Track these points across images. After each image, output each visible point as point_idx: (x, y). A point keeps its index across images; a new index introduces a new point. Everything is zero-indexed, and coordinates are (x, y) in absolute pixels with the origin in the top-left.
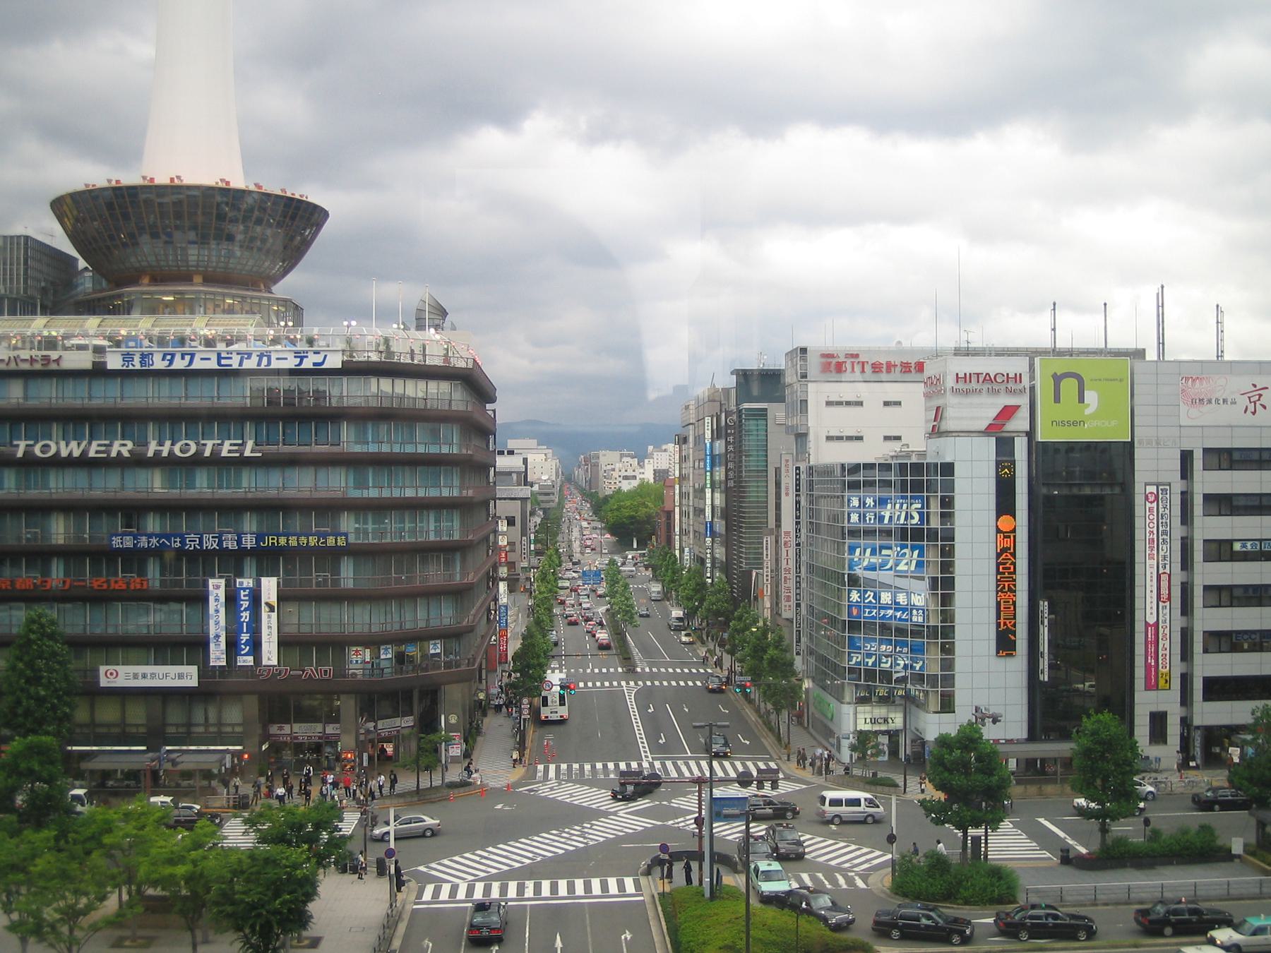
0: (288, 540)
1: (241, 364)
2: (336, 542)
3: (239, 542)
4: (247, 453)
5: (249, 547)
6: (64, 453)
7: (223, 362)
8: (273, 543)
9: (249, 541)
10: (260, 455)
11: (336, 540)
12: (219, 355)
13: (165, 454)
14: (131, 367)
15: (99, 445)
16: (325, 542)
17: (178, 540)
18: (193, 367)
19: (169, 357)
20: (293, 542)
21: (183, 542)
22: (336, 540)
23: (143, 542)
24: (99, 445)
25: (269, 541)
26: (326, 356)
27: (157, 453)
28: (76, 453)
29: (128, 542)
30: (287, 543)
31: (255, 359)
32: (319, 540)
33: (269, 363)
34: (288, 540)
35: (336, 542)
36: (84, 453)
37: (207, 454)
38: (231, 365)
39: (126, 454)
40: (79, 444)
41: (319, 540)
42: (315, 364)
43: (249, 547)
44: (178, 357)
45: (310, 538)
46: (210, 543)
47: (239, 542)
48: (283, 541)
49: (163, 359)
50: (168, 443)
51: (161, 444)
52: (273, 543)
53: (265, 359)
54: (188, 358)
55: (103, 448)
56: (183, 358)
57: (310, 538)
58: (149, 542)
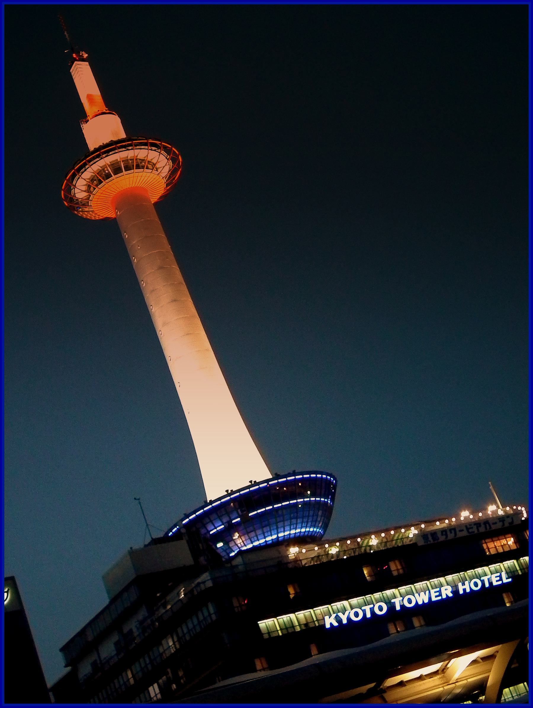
1: (478, 530)
4: (505, 581)
6: (420, 603)
7: (470, 530)
10: (510, 580)
12: (466, 526)
13: (468, 590)
14: (429, 543)
15: (435, 592)
18: (457, 536)
19: (444, 533)
24: (435, 592)
26: (512, 518)
27: (464, 590)
28: (426, 601)
31: (483, 526)
33: (490, 528)
36: (430, 598)
38: (474, 532)
39: (451, 595)
42: (510, 523)
44: (448, 533)
49: (442, 535)
50: (467, 583)
51: (463, 584)
53: (488, 527)
54: (453, 531)
55: (438, 594)
56: (451, 533)
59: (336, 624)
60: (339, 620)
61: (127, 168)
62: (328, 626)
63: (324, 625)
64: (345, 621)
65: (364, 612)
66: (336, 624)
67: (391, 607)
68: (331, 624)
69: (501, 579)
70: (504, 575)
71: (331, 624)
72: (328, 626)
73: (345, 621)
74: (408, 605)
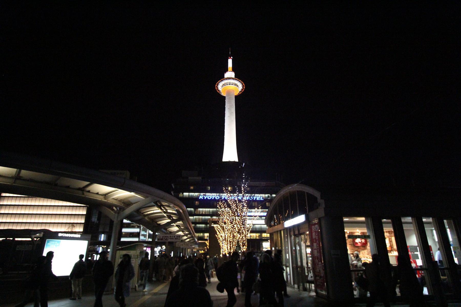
10: (263, 200)
37: (254, 199)
40: (233, 197)
59: (202, 198)
60: (204, 198)
61: (232, 84)
62: (200, 198)
63: (199, 198)
64: (205, 198)
65: (212, 197)
66: (202, 198)
67: (221, 198)
68: (201, 198)
69: (260, 199)
70: (261, 198)
71: (201, 198)
72: (200, 198)
73: (205, 198)
74: (216, 198)
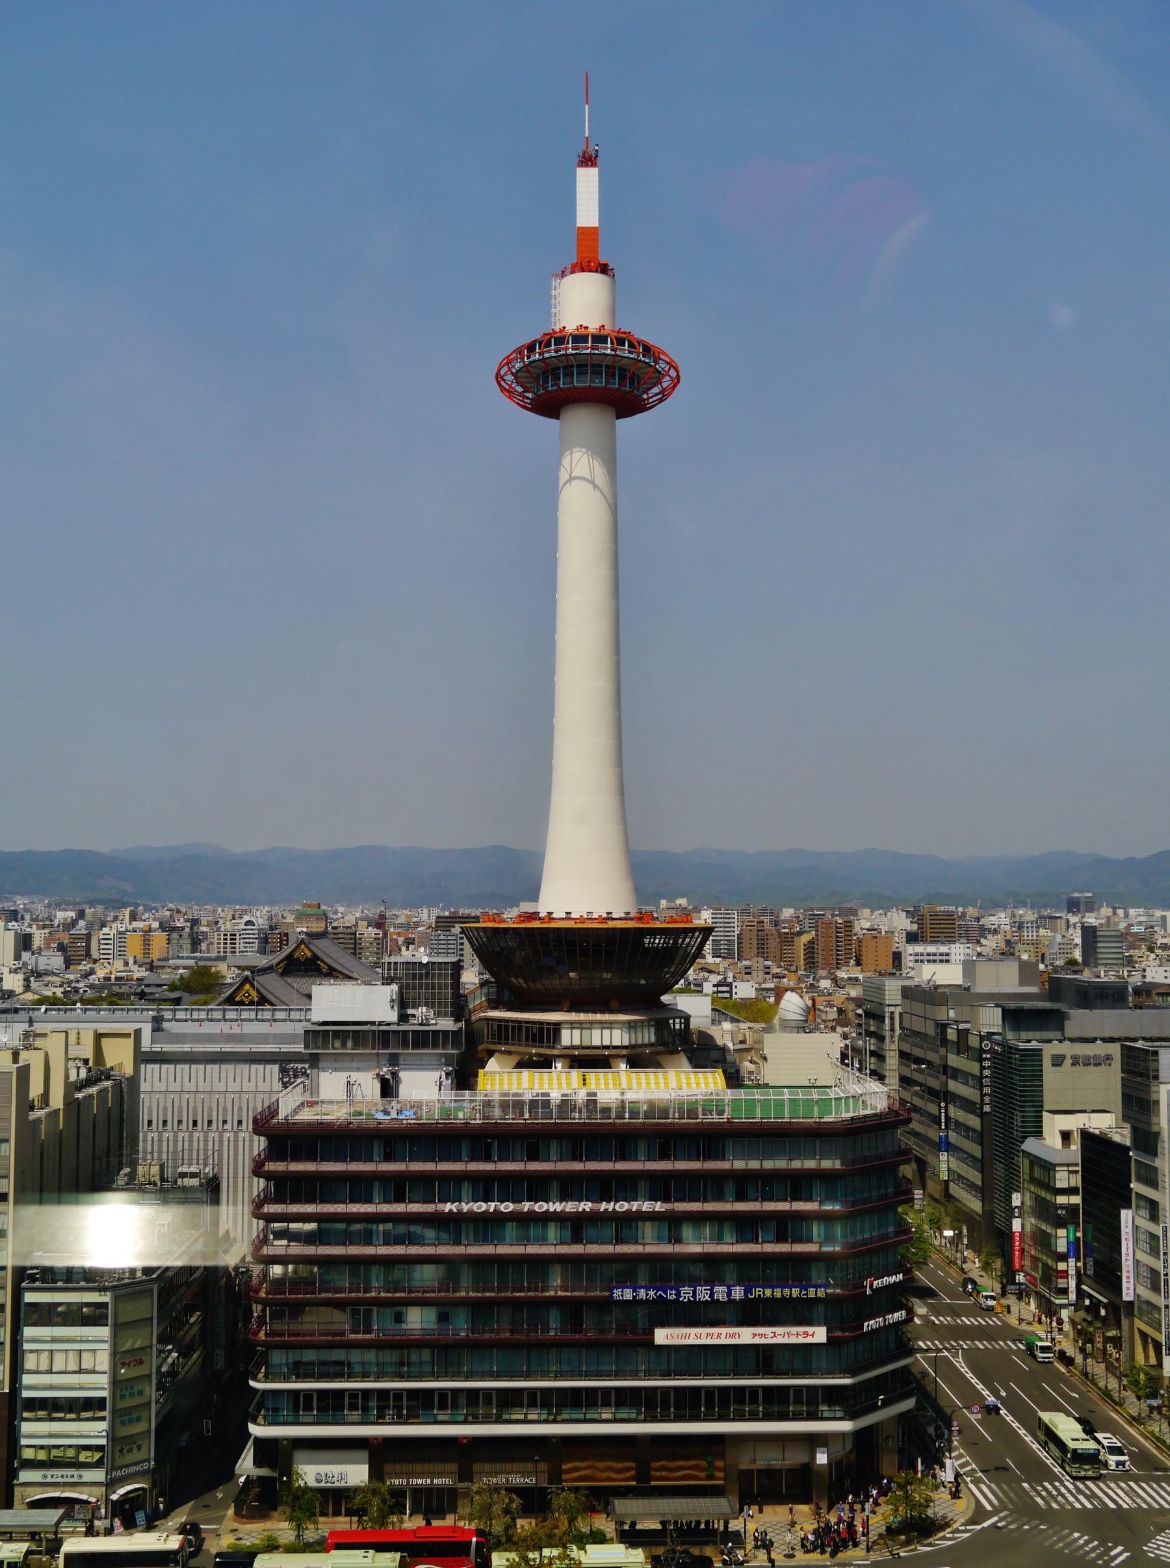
0: (773, 1292)
2: (816, 1294)
3: (729, 1294)
5: (738, 1298)
8: (759, 1295)
9: (738, 1293)
11: (816, 1292)
16: (807, 1294)
17: (674, 1292)
20: (778, 1293)
21: (678, 1295)
22: (816, 1292)
23: (642, 1294)
25: (757, 1292)
29: (628, 1294)
30: (773, 1295)
32: (801, 1292)
34: (773, 1292)
35: (816, 1294)
41: (801, 1292)
43: (738, 1298)
45: (793, 1290)
46: (703, 1294)
47: (729, 1294)
48: (768, 1293)
52: (759, 1295)
57: (793, 1290)
58: (647, 1295)
